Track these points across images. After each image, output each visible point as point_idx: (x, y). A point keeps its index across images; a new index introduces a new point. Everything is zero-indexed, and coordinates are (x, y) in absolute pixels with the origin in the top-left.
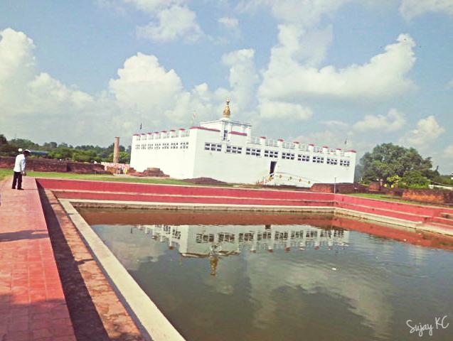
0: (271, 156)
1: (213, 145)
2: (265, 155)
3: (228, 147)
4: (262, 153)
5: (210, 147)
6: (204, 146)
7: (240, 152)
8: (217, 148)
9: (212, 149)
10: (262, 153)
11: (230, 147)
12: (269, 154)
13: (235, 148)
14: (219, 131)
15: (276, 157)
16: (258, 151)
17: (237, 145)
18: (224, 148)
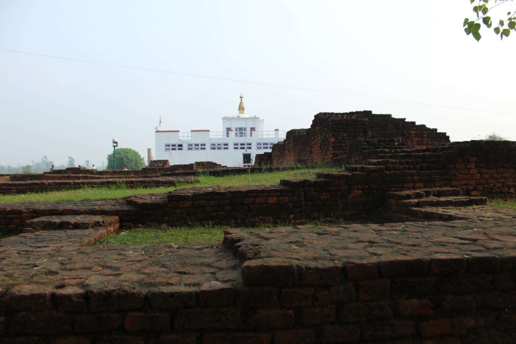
0: (241, 148)
1: (173, 145)
2: (235, 148)
3: (189, 145)
4: (231, 146)
5: (171, 147)
6: (164, 147)
7: (204, 149)
8: (177, 147)
9: (173, 149)
10: (231, 146)
11: (191, 145)
12: (239, 146)
13: (198, 145)
14: (179, 131)
15: (250, 148)
16: (225, 145)
17: (199, 142)
18: (185, 147)
